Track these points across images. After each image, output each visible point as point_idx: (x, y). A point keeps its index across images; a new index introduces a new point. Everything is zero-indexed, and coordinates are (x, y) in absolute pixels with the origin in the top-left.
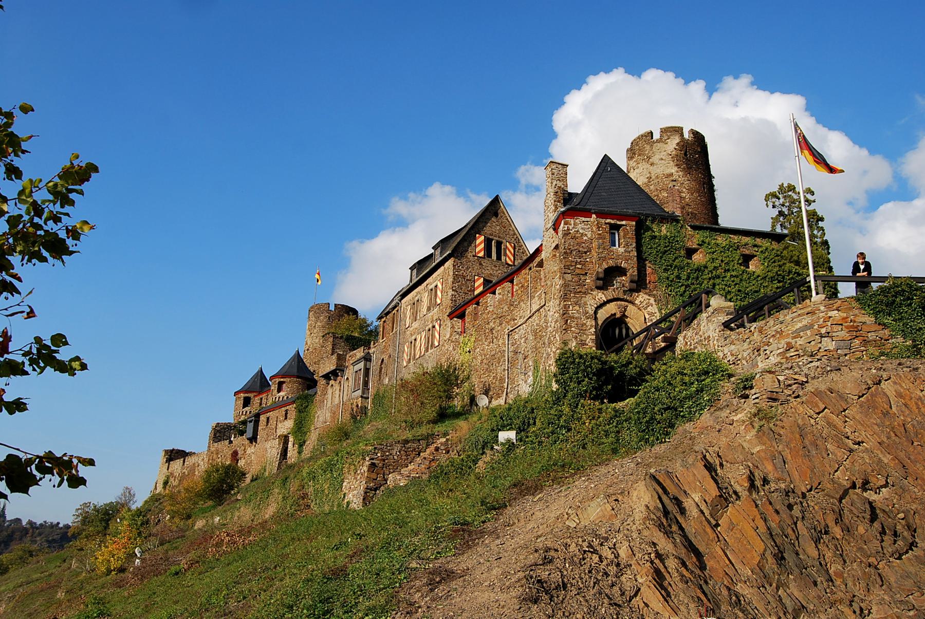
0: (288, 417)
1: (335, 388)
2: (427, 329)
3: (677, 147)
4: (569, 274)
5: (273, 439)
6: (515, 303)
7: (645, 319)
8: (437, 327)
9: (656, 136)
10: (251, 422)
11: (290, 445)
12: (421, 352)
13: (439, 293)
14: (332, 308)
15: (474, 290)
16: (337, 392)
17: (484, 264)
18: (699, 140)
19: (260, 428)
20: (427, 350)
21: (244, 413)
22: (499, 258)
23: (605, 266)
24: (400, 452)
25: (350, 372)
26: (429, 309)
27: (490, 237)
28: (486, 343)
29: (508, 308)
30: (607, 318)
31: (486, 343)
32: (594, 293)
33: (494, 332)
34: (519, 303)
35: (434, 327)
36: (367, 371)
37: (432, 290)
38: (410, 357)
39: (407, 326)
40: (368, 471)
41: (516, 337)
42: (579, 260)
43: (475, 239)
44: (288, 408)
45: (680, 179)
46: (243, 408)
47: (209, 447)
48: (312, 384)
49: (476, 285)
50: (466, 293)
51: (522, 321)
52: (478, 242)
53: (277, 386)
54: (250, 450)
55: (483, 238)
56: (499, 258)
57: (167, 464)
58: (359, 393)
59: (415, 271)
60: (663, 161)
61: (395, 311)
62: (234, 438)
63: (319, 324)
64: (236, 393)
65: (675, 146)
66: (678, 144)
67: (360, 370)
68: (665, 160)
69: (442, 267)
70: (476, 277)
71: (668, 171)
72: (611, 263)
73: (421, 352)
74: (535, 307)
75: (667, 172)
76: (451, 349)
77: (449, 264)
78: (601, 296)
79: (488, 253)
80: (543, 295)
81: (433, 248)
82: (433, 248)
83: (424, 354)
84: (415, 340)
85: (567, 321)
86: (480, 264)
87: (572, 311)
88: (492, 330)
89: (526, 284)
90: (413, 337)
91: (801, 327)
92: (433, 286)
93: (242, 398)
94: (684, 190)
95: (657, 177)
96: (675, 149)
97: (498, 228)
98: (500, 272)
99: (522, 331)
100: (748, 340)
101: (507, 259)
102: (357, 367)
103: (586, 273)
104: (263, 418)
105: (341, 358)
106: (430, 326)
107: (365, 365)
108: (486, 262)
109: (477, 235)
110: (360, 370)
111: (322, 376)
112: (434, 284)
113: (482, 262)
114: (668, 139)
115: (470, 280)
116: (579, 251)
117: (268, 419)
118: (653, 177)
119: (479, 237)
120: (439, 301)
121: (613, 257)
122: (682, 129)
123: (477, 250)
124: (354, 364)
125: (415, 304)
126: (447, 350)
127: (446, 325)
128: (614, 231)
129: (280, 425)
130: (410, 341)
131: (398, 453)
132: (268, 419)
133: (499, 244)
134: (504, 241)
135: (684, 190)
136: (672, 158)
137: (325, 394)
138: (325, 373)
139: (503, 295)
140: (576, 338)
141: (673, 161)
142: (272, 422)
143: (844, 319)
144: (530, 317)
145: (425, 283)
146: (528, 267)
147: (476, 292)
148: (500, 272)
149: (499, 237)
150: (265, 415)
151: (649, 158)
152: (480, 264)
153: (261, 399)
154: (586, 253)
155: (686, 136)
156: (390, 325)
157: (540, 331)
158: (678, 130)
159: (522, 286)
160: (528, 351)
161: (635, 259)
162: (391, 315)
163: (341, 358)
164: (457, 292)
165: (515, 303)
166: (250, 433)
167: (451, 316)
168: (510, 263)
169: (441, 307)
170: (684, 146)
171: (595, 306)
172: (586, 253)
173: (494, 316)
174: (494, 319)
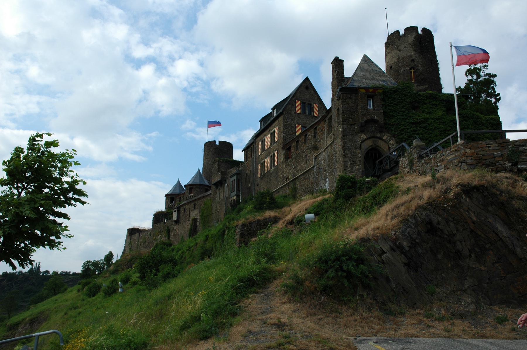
0: (196, 207)
1: (221, 191)
2: (270, 155)
3: (414, 39)
4: (345, 124)
5: (189, 220)
6: (318, 140)
7: (389, 147)
8: (276, 155)
9: (402, 32)
10: (175, 211)
11: (198, 223)
12: (268, 169)
13: (276, 135)
14: (217, 143)
15: (296, 133)
16: (222, 193)
17: (301, 117)
19: (181, 214)
20: (271, 168)
21: (171, 206)
23: (365, 119)
24: (256, 226)
25: (229, 182)
26: (271, 144)
27: (304, 101)
28: (303, 163)
29: (315, 143)
30: (368, 148)
31: (303, 163)
32: (360, 134)
33: (307, 157)
34: (320, 140)
35: (274, 154)
36: (238, 180)
37: (272, 133)
38: (262, 172)
39: (259, 154)
40: (240, 237)
41: (319, 159)
42: (351, 116)
43: (296, 103)
44: (195, 202)
45: (417, 59)
46: (170, 204)
47: (153, 226)
48: (208, 188)
49: (297, 129)
50: (291, 135)
51: (322, 150)
52: (297, 105)
53: (188, 190)
54: (176, 227)
55: (299, 102)
57: (130, 237)
58: (235, 193)
59: (263, 123)
60: (406, 49)
61: (252, 146)
62: (167, 220)
63: (210, 153)
64: (166, 196)
65: (413, 38)
66: (415, 37)
67: (235, 180)
68: (407, 47)
69: (277, 121)
70: (297, 125)
71: (409, 54)
72: (369, 117)
73: (268, 169)
74: (329, 143)
75: (408, 55)
76: (284, 167)
77: (281, 119)
78: (364, 136)
80: (333, 136)
81: (272, 109)
82: (272, 109)
83: (270, 170)
84: (264, 162)
85: (345, 151)
86: (299, 117)
88: (306, 156)
89: (323, 130)
90: (263, 161)
91: (452, 158)
92: (272, 131)
93: (169, 198)
95: (403, 58)
96: (413, 40)
97: (308, 96)
98: (310, 121)
99: (322, 157)
100: (429, 164)
101: (314, 113)
102: (233, 179)
103: (355, 124)
104: (182, 209)
105: (224, 174)
106: (272, 154)
107: (237, 177)
109: (296, 101)
110: (235, 180)
111: (213, 184)
112: (273, 130)
113: (300, 116)
114: (409, 35)
115: (293, 127)
116: (351, 111)
117: (185, 209)
118: (401, 58)
119: (297, 102)
120: (276, 140)
121: (369, 113)
122: (417, 28)
123: (297, 109)
124: (231, 177)
125: (263, 142)
126: (282, 167)
127: (281, 153)
128: (370, 99)
129: (191, 213)
130: (261, 162)
131: (256, 227)
132: (185, 209)
134: (312, 103)
136: (412, 46)
137: (216, 194)
138: (215, 182)
139: (311, 136)
140: (350, 160)
141: (412, 48)
142: (187, 212)
143: (473, 153)
144: (326, 148)
145: (268, 130)
146: (324, 120)
147: (297, 134)
148: (310, 121)
149: (310, 101)
150: (183, 208)
151: (398, 46)
152: (299, 117)
153: (180, 198)
154: (354, 112)
155: (420, 32)
156: (250, 154)
157: (332, 156)
158: (415, 29)
159: (322, 131)
160: (326, 168)
161: (382, 115)
162: (250, 148)
163: (224, 174)
164: (286, 134)
165: (318, 140)
166: (175, 218)
167: (283, 148)
168: (316, 115)
169: (278, 143)
171: (361, 141)
172: (354, 112)
173: (307, 148)
174: (307, 149)
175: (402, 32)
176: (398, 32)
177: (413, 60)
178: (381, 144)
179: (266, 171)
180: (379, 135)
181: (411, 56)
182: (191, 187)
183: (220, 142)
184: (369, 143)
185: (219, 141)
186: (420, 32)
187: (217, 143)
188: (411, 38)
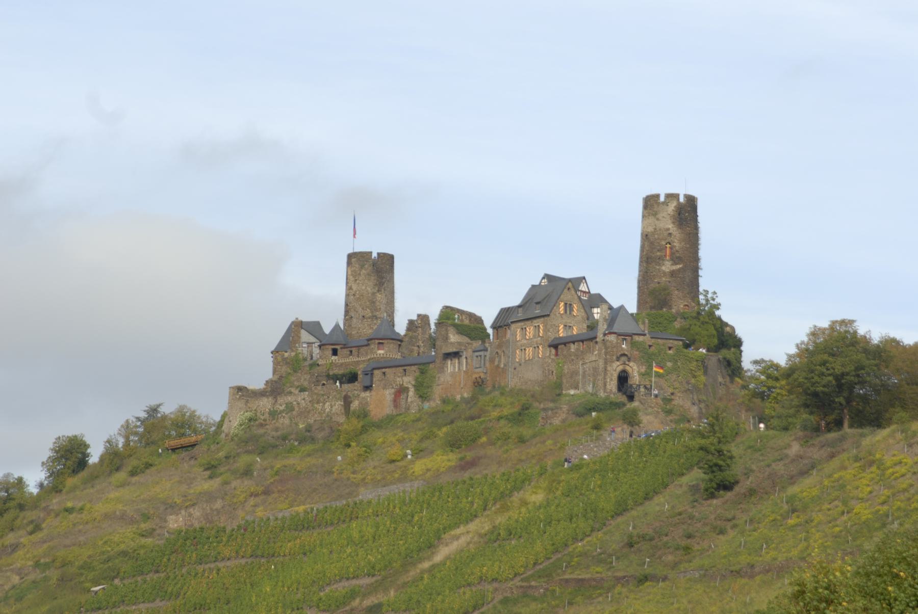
9: (662, 199)
18: (691, 202)
22: (570, 313)
56: (570, 313)
65: (673, 208)
66: (675, 207)
78: (618, 363)
79: (566, 312)
87: (609, 368)
94: (676, 241)
99: (588, 365)
108: (564, 316)
133: (571, 305)
135: (676, 241)
155: (682, 199)
170: (680, 209)
175: (662, 199)
176: (658, 196)
177: (670, 234)
178: (628, 368)
179: (527, 359)
180: (627, 363)
181: (668, 229)
182: (381, 341)
183: (379, 254)
184: (621, 368)
185: (379, 254)
186: (682, 199)
187: (374, 255)
188: (672, 206)
